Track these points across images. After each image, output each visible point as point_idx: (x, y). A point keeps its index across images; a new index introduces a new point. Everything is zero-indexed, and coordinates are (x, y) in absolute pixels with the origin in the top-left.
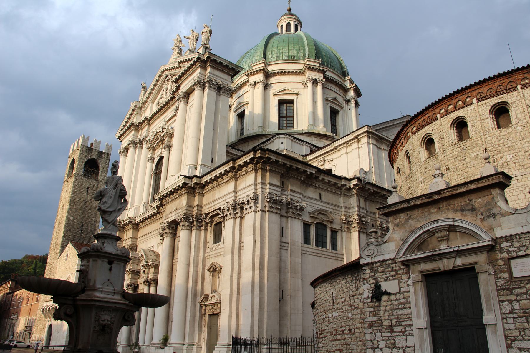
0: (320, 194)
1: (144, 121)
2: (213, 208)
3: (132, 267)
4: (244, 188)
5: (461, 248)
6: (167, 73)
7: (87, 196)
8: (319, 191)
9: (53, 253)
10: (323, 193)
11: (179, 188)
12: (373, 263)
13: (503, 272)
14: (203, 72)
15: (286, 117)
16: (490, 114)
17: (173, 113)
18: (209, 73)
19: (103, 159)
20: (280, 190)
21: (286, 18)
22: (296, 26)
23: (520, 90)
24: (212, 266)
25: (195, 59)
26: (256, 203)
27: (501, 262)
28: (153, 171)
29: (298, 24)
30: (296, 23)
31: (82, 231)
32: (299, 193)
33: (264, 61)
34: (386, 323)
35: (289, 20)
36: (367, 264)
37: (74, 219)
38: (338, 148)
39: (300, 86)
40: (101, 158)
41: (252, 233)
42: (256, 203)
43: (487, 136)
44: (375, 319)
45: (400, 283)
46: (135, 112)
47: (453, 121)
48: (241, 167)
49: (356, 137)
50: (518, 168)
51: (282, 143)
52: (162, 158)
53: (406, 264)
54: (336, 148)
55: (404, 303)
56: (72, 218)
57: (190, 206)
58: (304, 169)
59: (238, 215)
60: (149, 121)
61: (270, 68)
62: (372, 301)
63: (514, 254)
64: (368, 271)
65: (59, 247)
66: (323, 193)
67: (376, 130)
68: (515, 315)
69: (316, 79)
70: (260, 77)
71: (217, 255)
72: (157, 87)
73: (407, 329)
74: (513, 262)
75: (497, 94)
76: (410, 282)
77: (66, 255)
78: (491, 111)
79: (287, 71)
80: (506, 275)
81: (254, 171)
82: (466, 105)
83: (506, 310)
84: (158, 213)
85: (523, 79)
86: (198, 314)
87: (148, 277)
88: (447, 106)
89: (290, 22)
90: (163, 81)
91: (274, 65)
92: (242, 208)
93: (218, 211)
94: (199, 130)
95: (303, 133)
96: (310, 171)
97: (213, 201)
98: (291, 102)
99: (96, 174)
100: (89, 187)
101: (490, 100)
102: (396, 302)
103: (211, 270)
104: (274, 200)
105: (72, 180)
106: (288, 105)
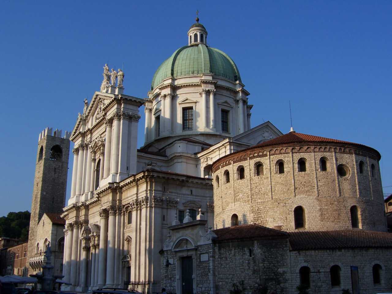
0: (191, 191)
1: (87, 131)
2: (127, 202)
3: (85, 236)
4: (141, 192)
5: (188, 249)
6: (100, 97)
7: (55, 175)
8: (190, 189)
9: (33, 220)
10: (194, 190)
11: (107, 189)
12: (168, 250)
13: (198, 259)
14: (119, 107)
15: (189, 120)
16: (237, 171)
17: (104, 130)
18: (123, 108)
19: (65, 144)
20: (162, 193)
21: (194, 30)
22: (202, 36)
23: (248, 160)
24: (127, 238)
25: (113, 99)
26: (147, 202)
27: (198, 255)
28: (96, 169)
29: (203, 34)
30: (202, 33)
31: (53, 202)
32: (175, 193)
33: (171, 77)
34: (170, 276)
35: (196, 31)
36: (166, 251)
37: (47, 194)
38: (215, 151)
39: (198, 94)
40: (63, 144)
41: (145, 220)
42: (147, 202)
43: (235, 183)
44: (166, 274)
45: (174, 260)
46: (81, 123)
47: (225, 171)
48: (138, 180)
49: (223, 145)
50: (244, 202)
51: (180, 146)
52: (100, 160)
53: (176, 252)
54: (213, 151)
55: (173, 269)
56: (45, 193)
57: (114, 200)
58: (177, 178)
59: (139, 208)
60: (91, 131)
61: (177, 83)
62: (166, 267)
63: (201, 253)
64: (166, 254)
65: (37, 216)
66: (194, 190)
67: (235, 140)
68: (199, 275)
69: (209, 90)
70: (168, 91)
71: (130, 231)
72: (94, 106)
73: (175, 279)
74: (201, 255)
75: (240, 160)
76: (176, 260)
77: (43, 222)
78: (238, 169)
79: (188, 84)
80: (199, 260)
81: (145, 182)
82: (230, 164)
83: (198, 274)
84: (99, 200)
85: (250, 154)
86: (121, 266)
87: (94, 243)
88: (223, 162)
89: (197, 33)
90: (98, 102)
91: (179, 79)
92: (140, 204)
93: (129, 205)
94: (118, 149)
95: (198, 134)
96: (181, 178)
97: (127, 198)
98: (191, 108)
99: (60, 157)
100: (56, 168)
101: (237, 163)
102: (172, 268)
103: (127, 240)
104: (158, 200)
105: (42, 162)
106: (190, 111)
